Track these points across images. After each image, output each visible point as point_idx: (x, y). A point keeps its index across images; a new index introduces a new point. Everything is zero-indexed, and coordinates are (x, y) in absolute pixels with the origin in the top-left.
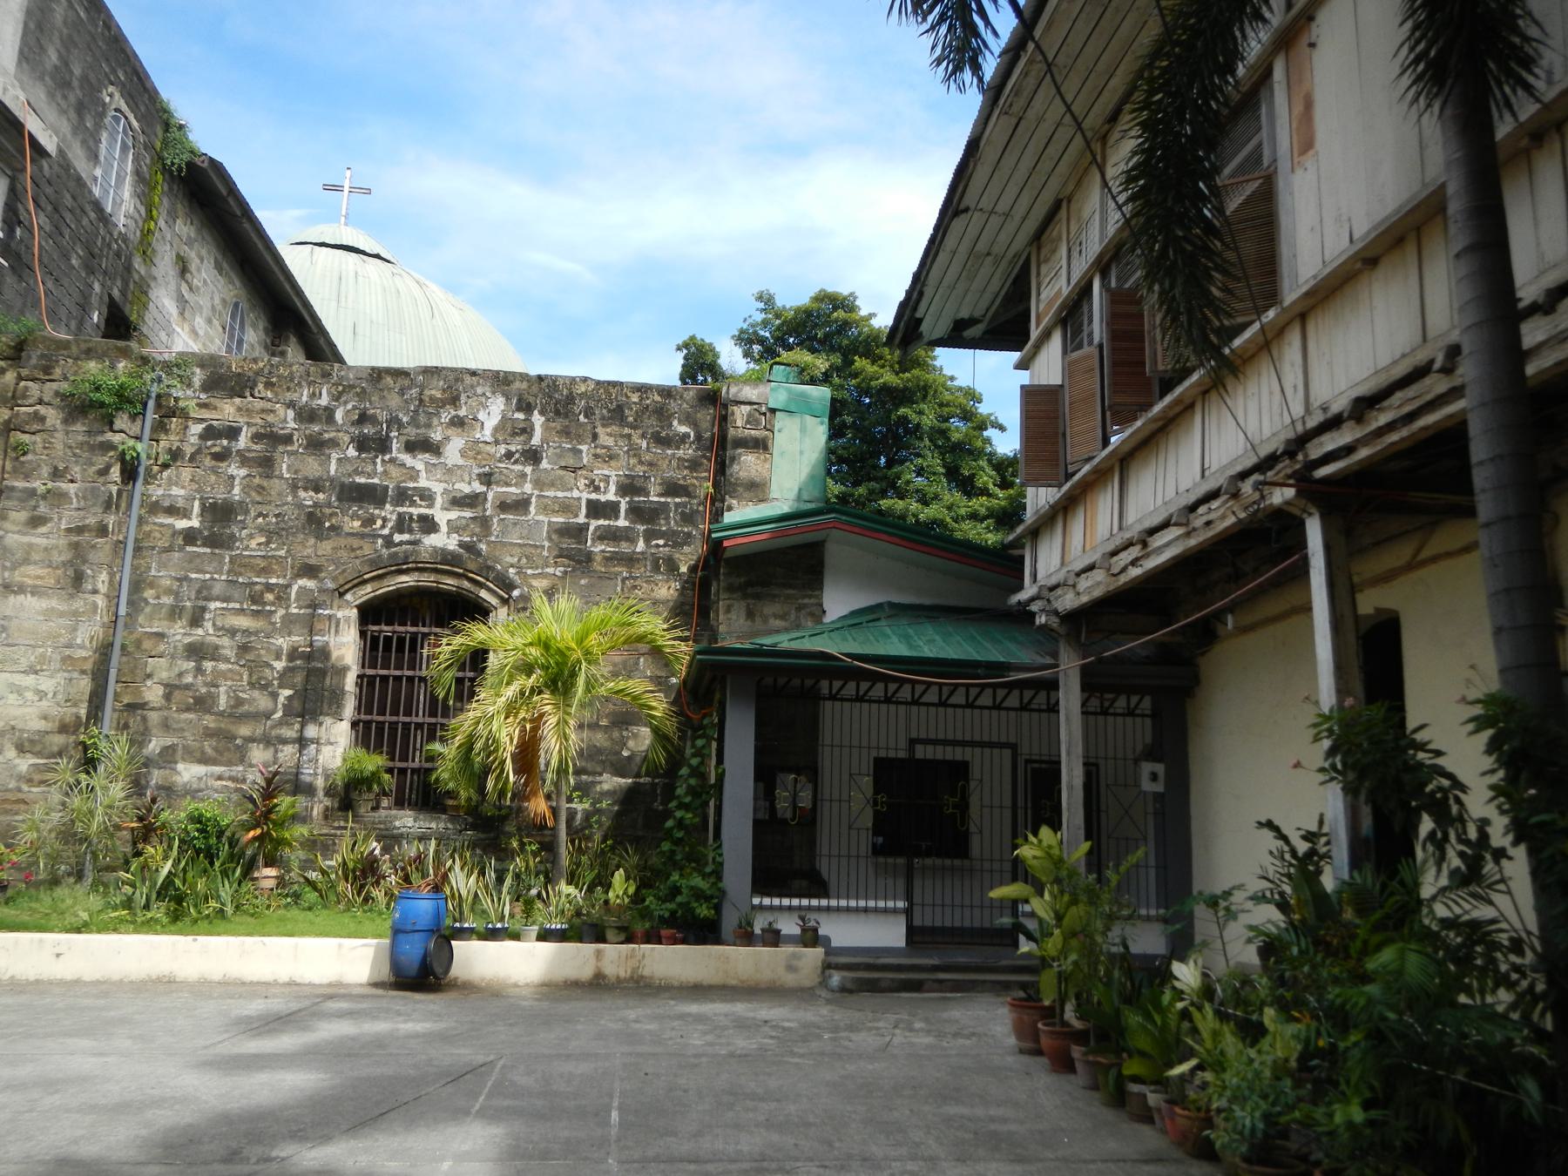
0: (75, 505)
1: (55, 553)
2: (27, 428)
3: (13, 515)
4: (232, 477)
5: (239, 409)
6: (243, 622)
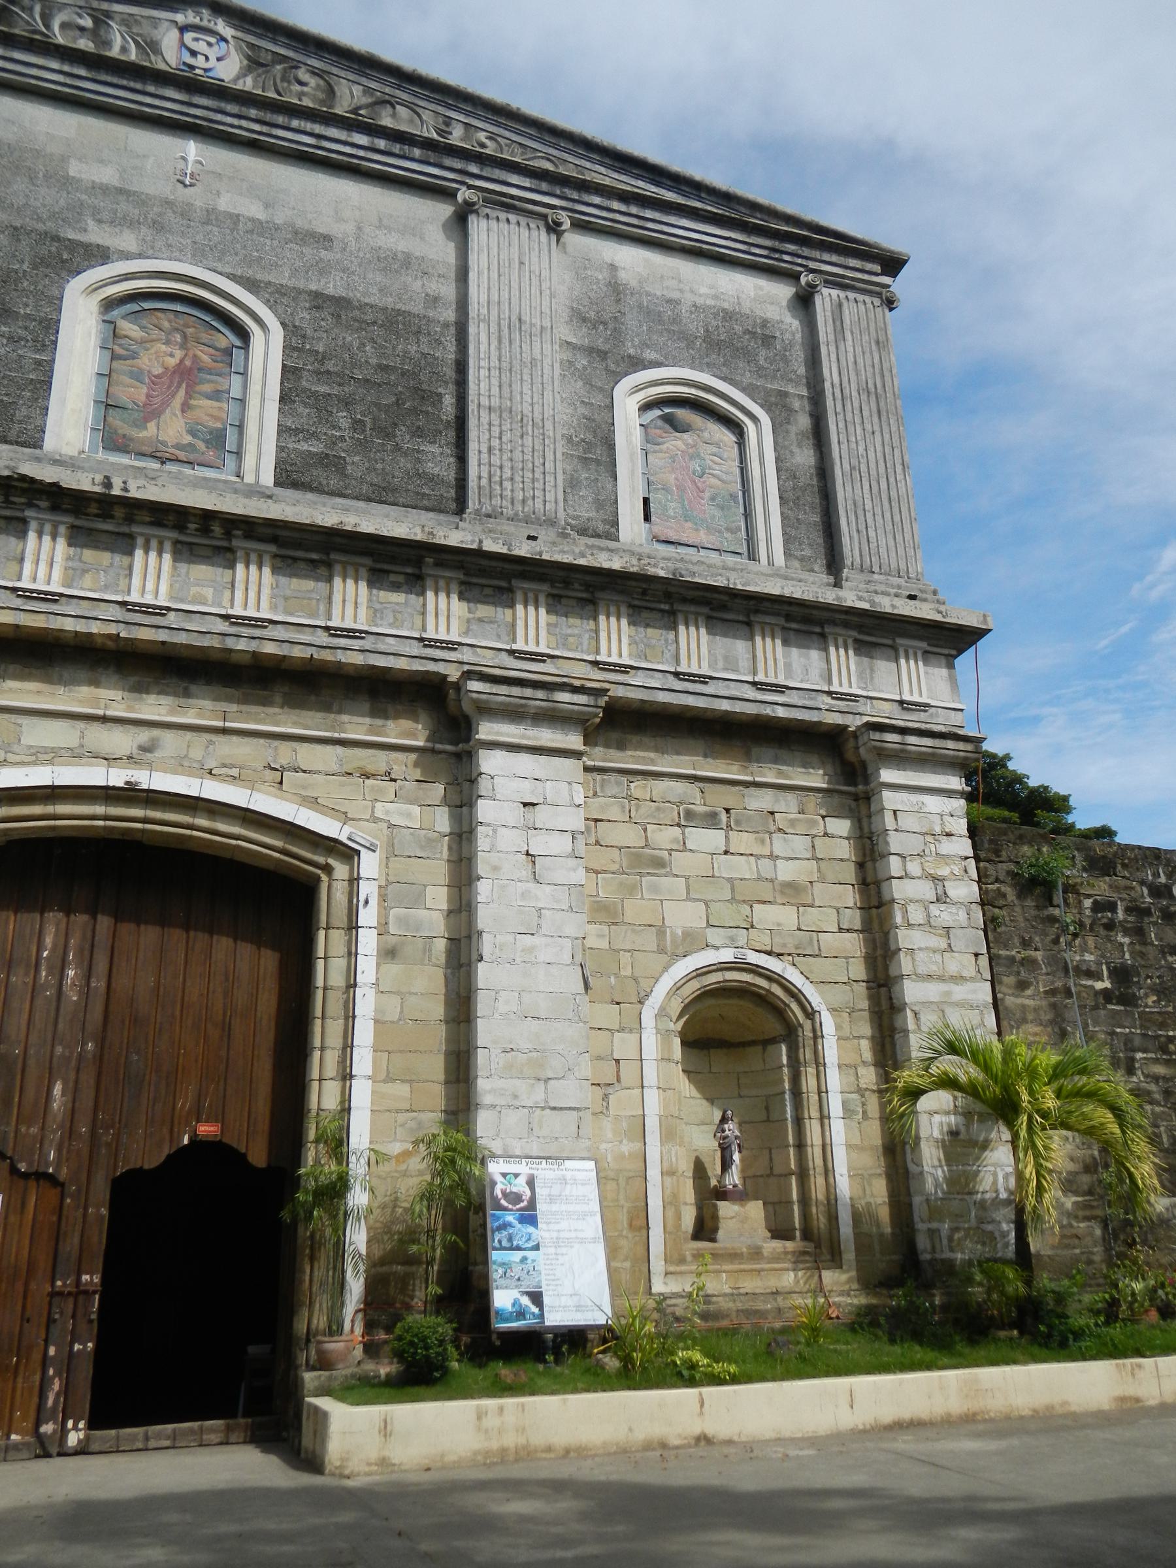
0: (1044, 971)
1: (1042, 1013)
2: (996, 903)
3: (1005, 979)
4: (1121, 945)
5: (1110, 886)
6: (1160, 1070)
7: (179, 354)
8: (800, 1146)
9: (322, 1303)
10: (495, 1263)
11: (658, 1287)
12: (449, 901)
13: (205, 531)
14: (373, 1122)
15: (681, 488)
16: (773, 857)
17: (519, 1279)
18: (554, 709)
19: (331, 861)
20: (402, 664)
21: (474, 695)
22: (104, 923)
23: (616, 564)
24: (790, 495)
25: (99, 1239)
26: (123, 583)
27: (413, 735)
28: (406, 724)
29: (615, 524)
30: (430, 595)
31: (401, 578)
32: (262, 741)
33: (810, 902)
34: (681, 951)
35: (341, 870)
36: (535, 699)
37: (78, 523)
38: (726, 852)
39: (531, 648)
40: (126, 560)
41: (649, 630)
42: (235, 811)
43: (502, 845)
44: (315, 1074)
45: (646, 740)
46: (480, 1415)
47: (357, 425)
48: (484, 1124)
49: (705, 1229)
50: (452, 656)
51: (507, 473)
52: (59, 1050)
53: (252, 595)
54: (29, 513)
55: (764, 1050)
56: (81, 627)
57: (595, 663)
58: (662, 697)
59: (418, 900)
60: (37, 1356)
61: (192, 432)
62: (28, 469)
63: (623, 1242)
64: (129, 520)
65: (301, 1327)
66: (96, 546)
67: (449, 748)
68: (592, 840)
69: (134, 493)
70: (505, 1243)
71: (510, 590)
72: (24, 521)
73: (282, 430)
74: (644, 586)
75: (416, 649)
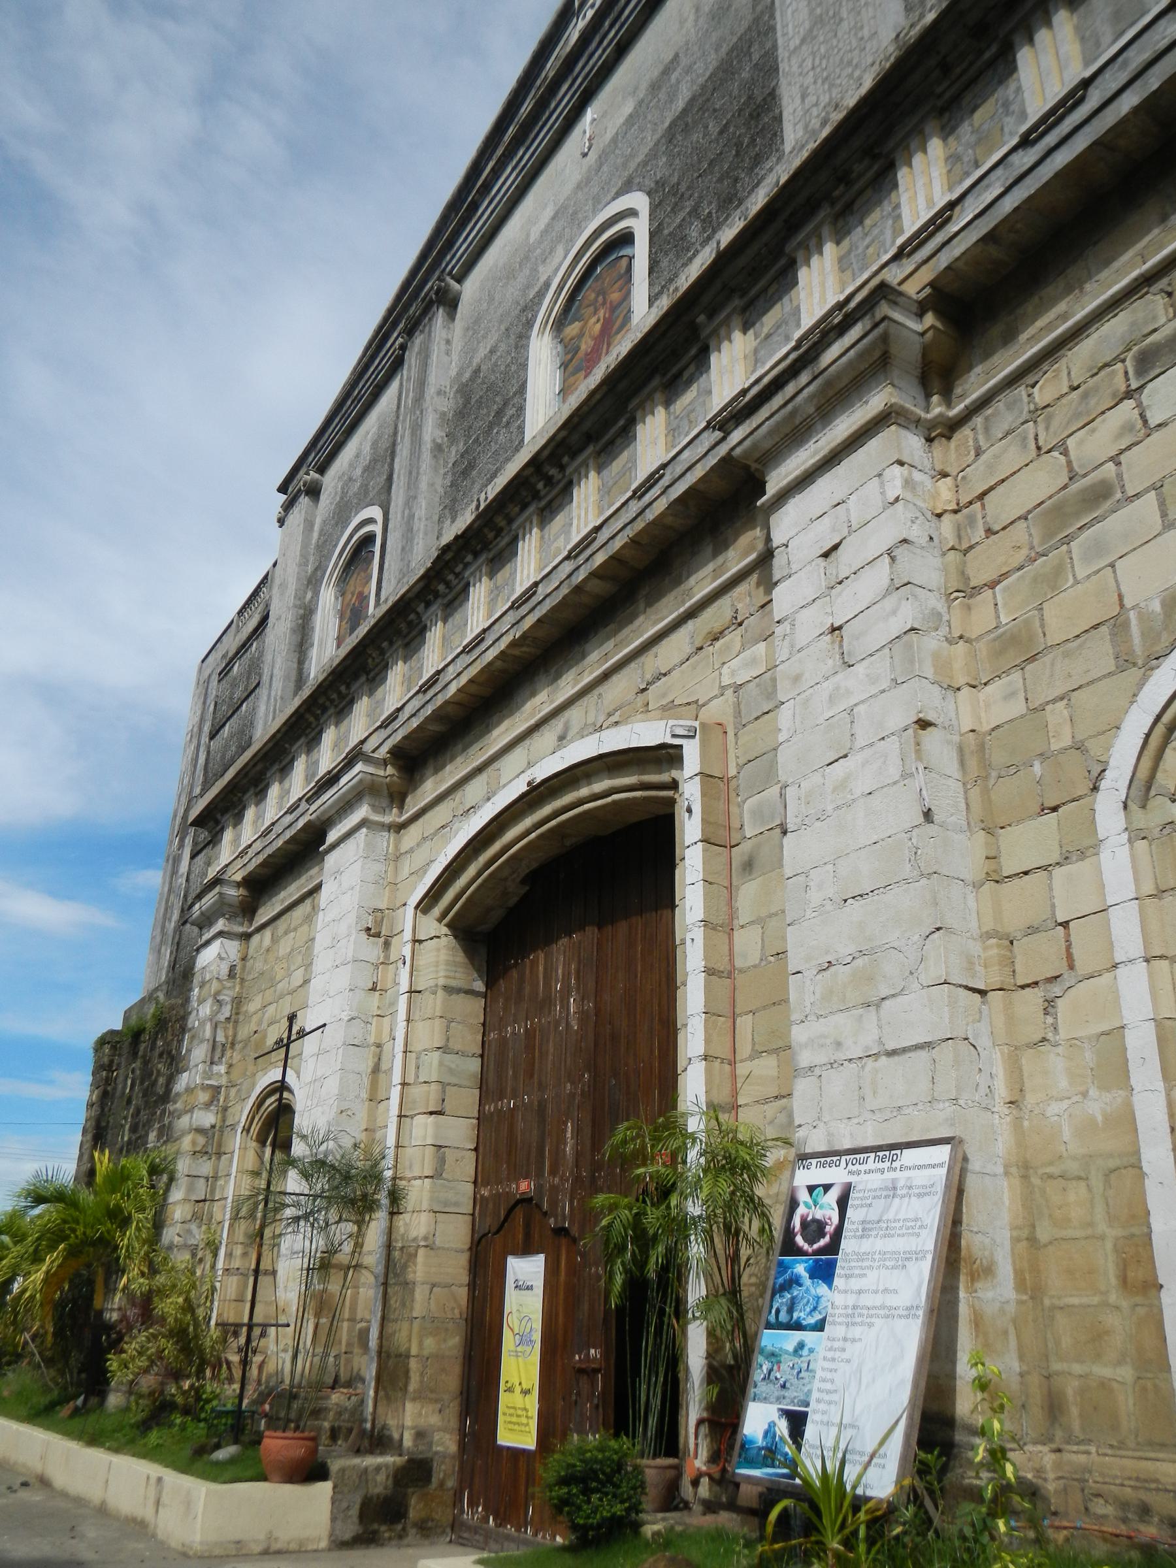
10: (762, 1352)
17: (784, 1386)
18: (829, 384)
22: (591, 932)
32: (633, 665)
42: (594, 764)
58: (1009, 204)
63: (1112, 1320)
70: (783, 1317)
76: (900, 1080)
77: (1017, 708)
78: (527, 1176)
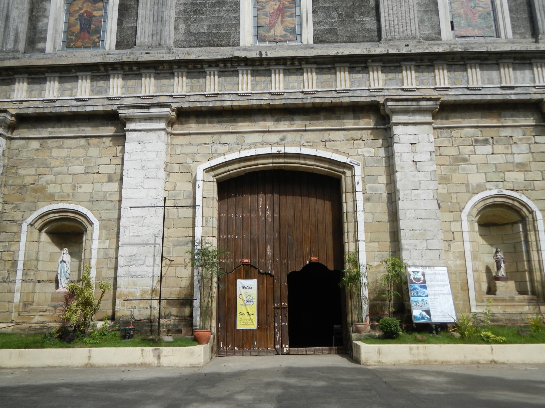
7: (278, 4)
8: (529, 261)
9: (355, 312)
11: (474, 310)
12: (387, 180)
13: (293, 64)
14: (367, 255)
15: (466, 14)
16: (512, 154)
18: (420, 108)
19: (345, 170)
20: (363, 99)
21: (390, 107)
22: (276, 196)
23: (441, 50)
24: (514, 8)
25: (286, 292)
26: (269, 86)
27: (369, 124)
28: (366, 120)
29: (440, 34)
30: (371, 73)
31: (360, 69)
32: (318, 132)
33: (529, 169)
34: (476, 191)
35: (348, 173)
36: (412, 105)
37: (254, 68)
38: (492, 154)
39: (410, 86)
40: (269, 78)
41: (456, 73)
43: (404, 159)
44: (346, 240)
45: (457, 115)
46: (411, 349)
47: (340, 16)
48: (405, 255)
49: (491, 290)
50: (381, 94)
51: (396, 22)
52: (267, 236)
53: (310, 83)
54: (239, 68)
55: (512, 226)
56: (258, 103)
57: (435, 89)
59: (376, 181)
60: (272, 326)
61: (285, 30)
62: (237, 54)
64: (269, 65)
65: (349, 319)
66: (260, 75)
67: (382, 127)
68: (438, 154)
69: (269, 56)
71: (400, 66)
72: (238, 71)
73: (315, 23)
74: (453, 56)
75: (367, 93)
76: (431, 254)
77: (445, 191)
78: (247, 258)
